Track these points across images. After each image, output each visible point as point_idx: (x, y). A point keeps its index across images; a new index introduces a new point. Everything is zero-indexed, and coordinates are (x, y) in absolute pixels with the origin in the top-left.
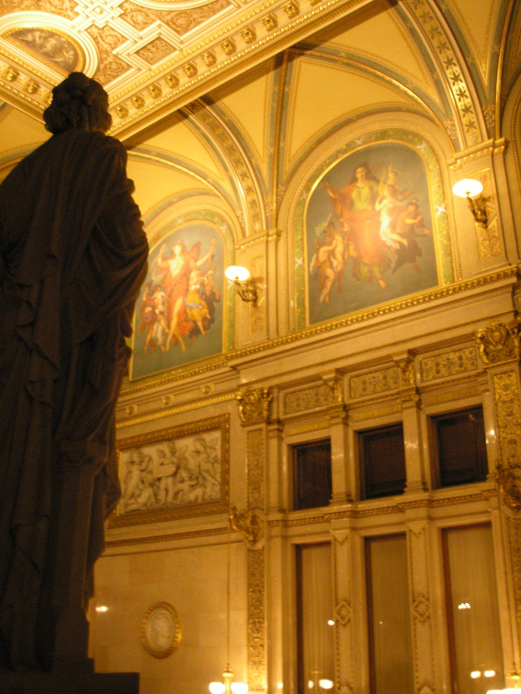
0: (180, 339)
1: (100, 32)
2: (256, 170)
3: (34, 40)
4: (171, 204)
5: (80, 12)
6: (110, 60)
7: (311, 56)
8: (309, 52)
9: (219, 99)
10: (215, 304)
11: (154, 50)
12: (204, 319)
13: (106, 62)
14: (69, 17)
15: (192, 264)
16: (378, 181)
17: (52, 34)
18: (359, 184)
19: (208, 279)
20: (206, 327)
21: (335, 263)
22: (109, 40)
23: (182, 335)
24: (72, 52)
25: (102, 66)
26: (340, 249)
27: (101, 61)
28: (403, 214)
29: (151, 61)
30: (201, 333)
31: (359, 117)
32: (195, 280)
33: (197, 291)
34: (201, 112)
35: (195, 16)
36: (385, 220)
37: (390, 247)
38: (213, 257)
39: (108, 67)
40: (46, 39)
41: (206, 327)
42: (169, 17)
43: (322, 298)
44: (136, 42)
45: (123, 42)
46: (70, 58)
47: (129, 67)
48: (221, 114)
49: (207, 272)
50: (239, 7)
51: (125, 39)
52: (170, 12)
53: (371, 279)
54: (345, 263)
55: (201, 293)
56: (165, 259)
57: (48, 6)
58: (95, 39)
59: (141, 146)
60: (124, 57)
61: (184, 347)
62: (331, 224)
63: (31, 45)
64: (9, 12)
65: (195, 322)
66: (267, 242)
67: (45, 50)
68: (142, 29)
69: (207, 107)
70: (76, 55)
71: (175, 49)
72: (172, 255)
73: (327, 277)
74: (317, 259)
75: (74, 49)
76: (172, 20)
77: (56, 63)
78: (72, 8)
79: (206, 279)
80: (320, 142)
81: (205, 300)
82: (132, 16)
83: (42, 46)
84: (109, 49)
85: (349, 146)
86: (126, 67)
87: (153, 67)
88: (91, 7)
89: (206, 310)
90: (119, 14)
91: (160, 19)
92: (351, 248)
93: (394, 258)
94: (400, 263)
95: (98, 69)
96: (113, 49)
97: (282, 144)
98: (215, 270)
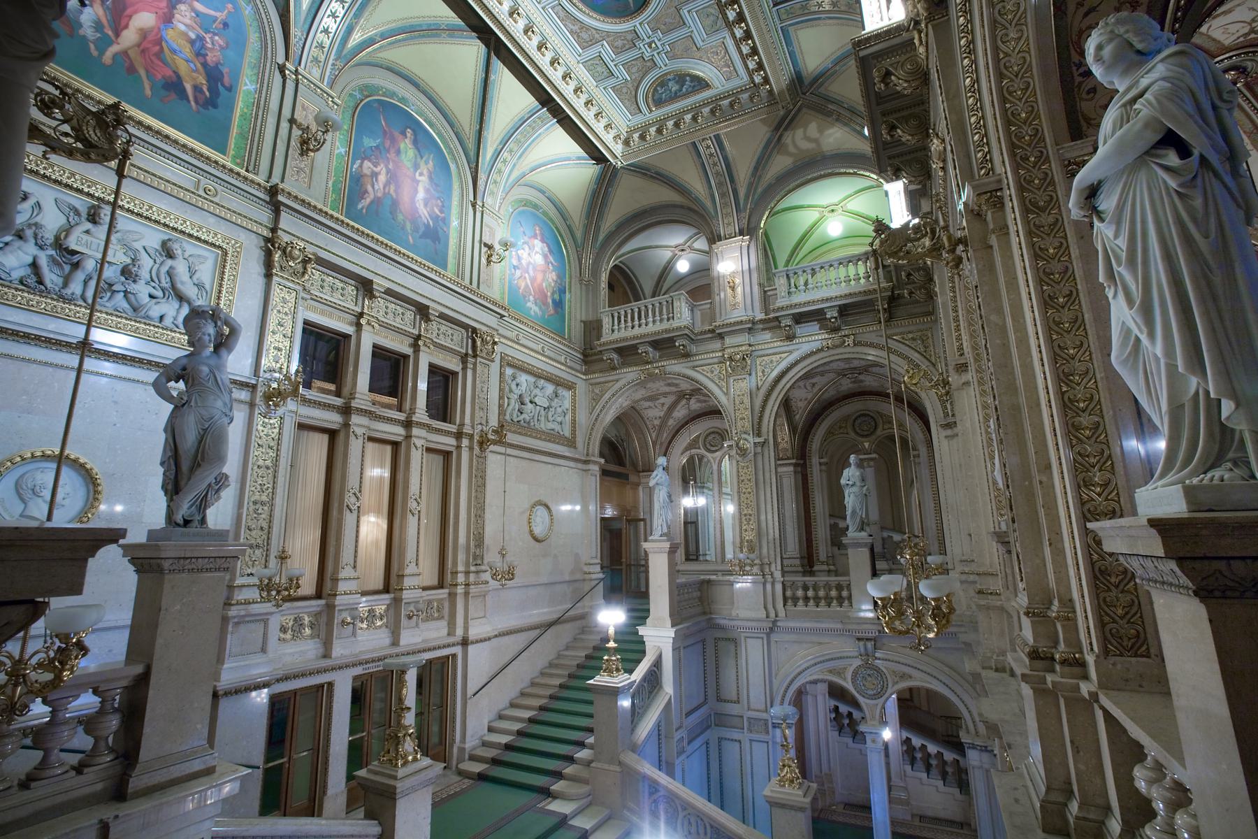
0: (142, 73)
12: (197, 89)
16: (422, 158)
18: (407, 141)
19: (213, 44)
20: (201, 102)
21: (376, 187)
23: (147, 71)
26: (382, 178)
28: (434, 201)
30: (189, 101)
31: (425, 93)
32: (188, 21)
33: (192, 42)
36: (421, 195)
37: (420, 216)
38: (226, 25)
41: (201, 102)
43: (360, 206)
49: (215, 34)
53: (403, 228)
54: (384, 193)
61: (148, 92)
62: (377, 147)
65: (179, 77)
73: (366, 192)
74: (361, 166)
79: (208, 40)
80: (389, 69)
81: (205, 65)
85: (403, 100)
89: (202, 80)
92: (392, 188)
93: (422, 229)
94: (424, 236)
98: (227, 44)
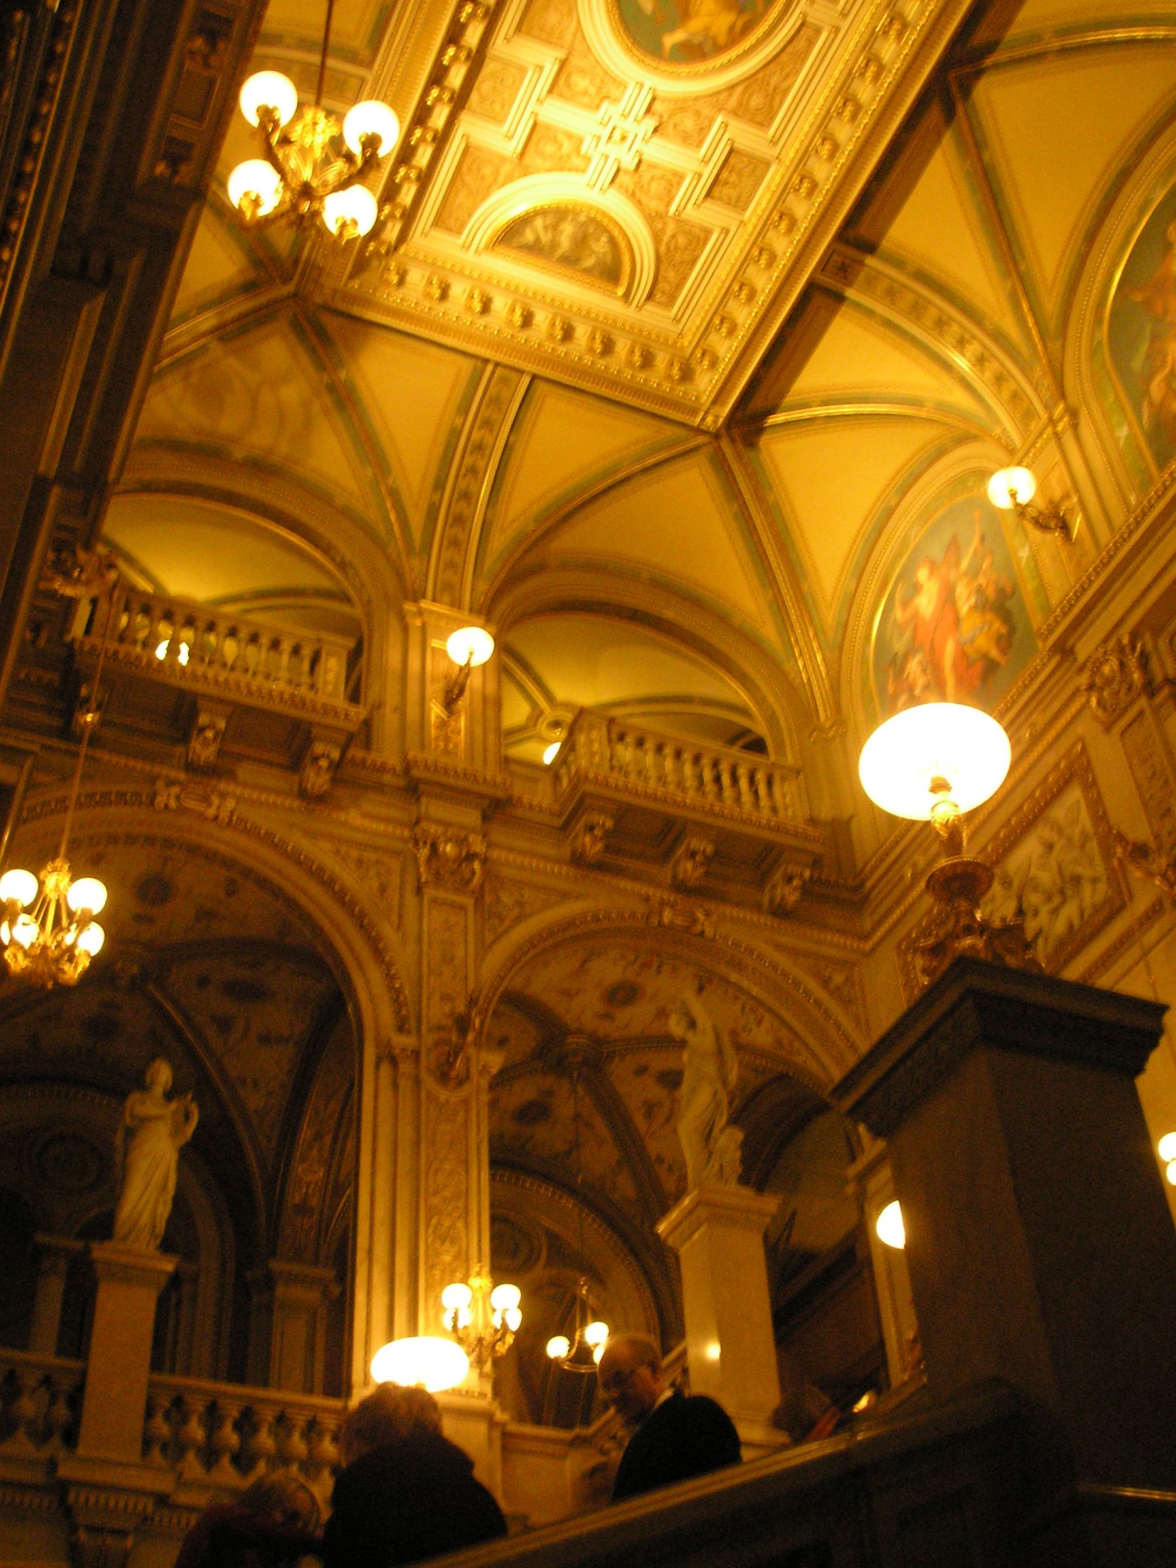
1: (637, 176)
2: (999, 337)
3: (538, 240)
4: (889, 513)
5: (591, 152)
6: (669, 231)
7: (997, 66)
8: (989, 61)
9: (881, 234)
10: (1010, 604)
11: (733, 178)
13: (666, 239)
14: (577, 170)
15: (953, 575)
17: (558, 214)
22: (654, 187)
24: (604, 239)
25: (663, 249)
27: (657, 238)
29: (739, 204)
34: (862, 276)
35: (774, 81)
39: (672, 245)
40: (555, 227)
42: (733, 102)
44: (700, 176)
45: (679, 184)
46: (604, 254)
47: (708, 232)
48: (898, 263)
50: (837, 30)
51: (680, 177)
52: (731, 88)
55: (982, 606)
56: (906, 604)
57: (539, 161)
58: (633, 195)
59: (788, 400)
60: (691, 213)
63: (535, 249)
64: (484, 198)
66: (1057, 436)
67: (560, 252)
68: (700, 144)
69: (870, 261)
70: (612, 242)
71: (768, 165)
72: (917, 588)
75: (606, 230)
76: (740, 104)
77: (588, 271)
78: (578, 151)
82: (675, 126)
83: (554, 245)
84: (661, 208)
86: (702, 236)
87: (748, 214)
88: (605, 134)
90: (651, 130)
91: (720, 110)
95: (658, 259)
96: (669, 204)
97: (1022, 268)
